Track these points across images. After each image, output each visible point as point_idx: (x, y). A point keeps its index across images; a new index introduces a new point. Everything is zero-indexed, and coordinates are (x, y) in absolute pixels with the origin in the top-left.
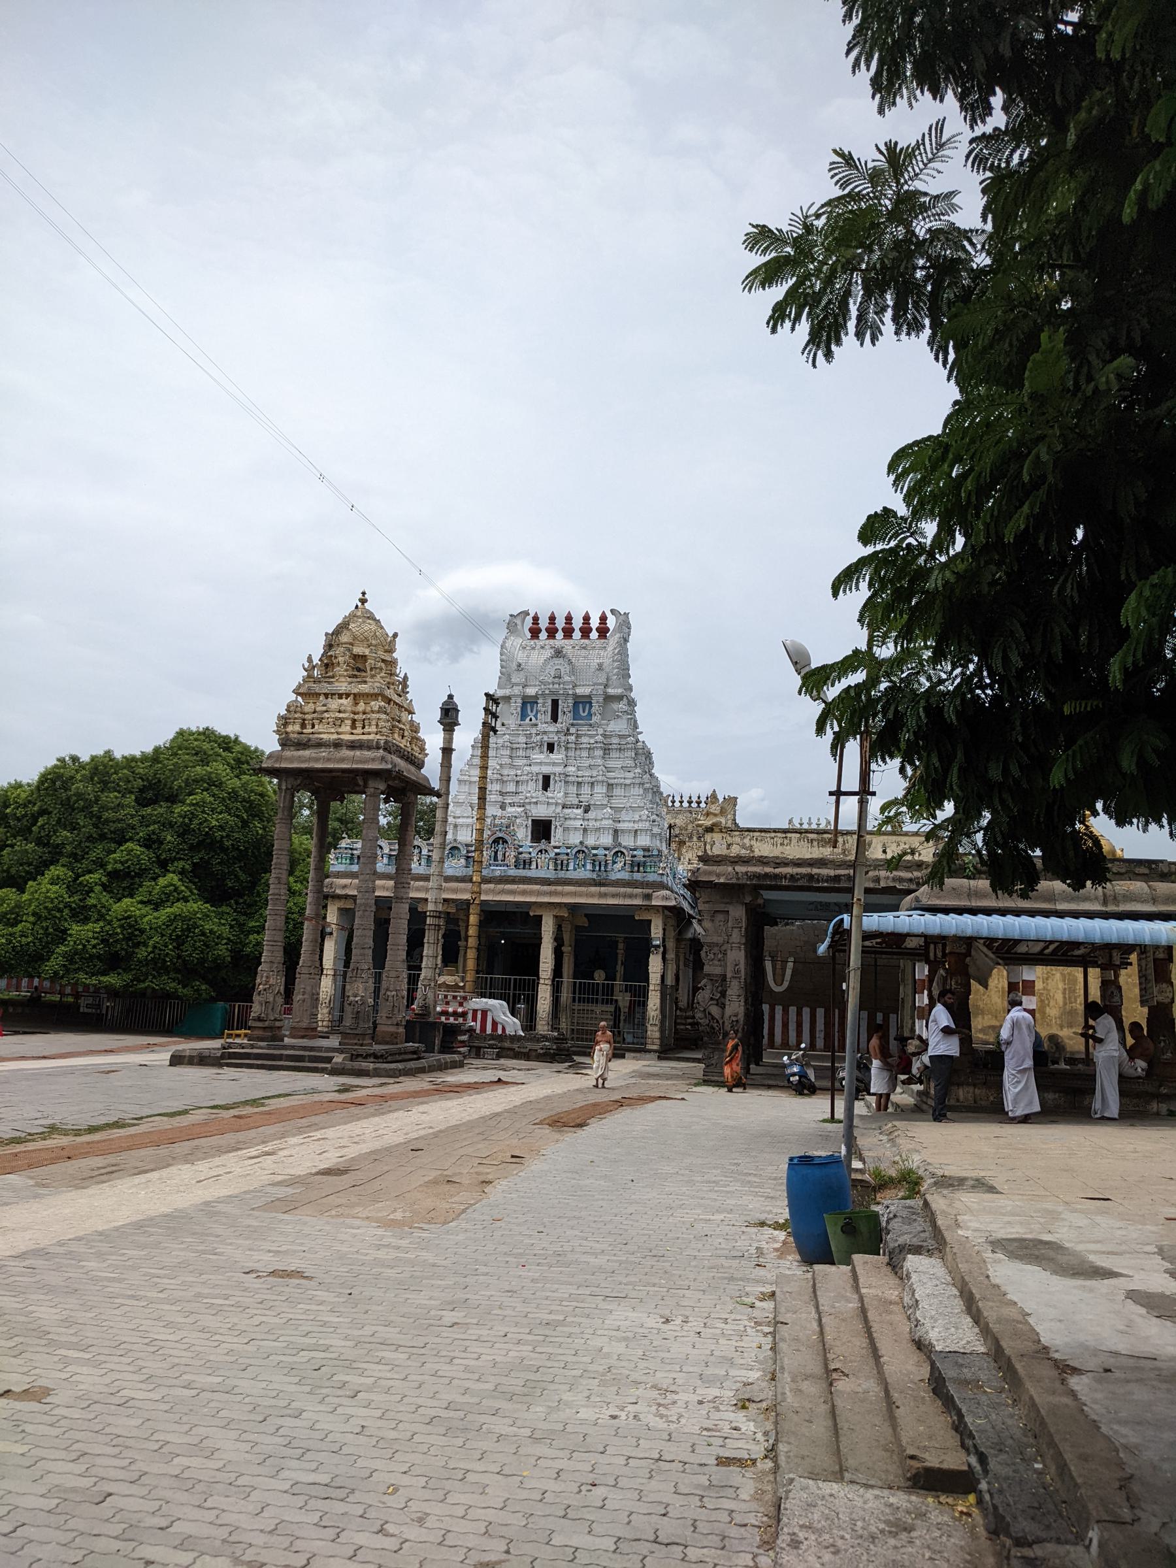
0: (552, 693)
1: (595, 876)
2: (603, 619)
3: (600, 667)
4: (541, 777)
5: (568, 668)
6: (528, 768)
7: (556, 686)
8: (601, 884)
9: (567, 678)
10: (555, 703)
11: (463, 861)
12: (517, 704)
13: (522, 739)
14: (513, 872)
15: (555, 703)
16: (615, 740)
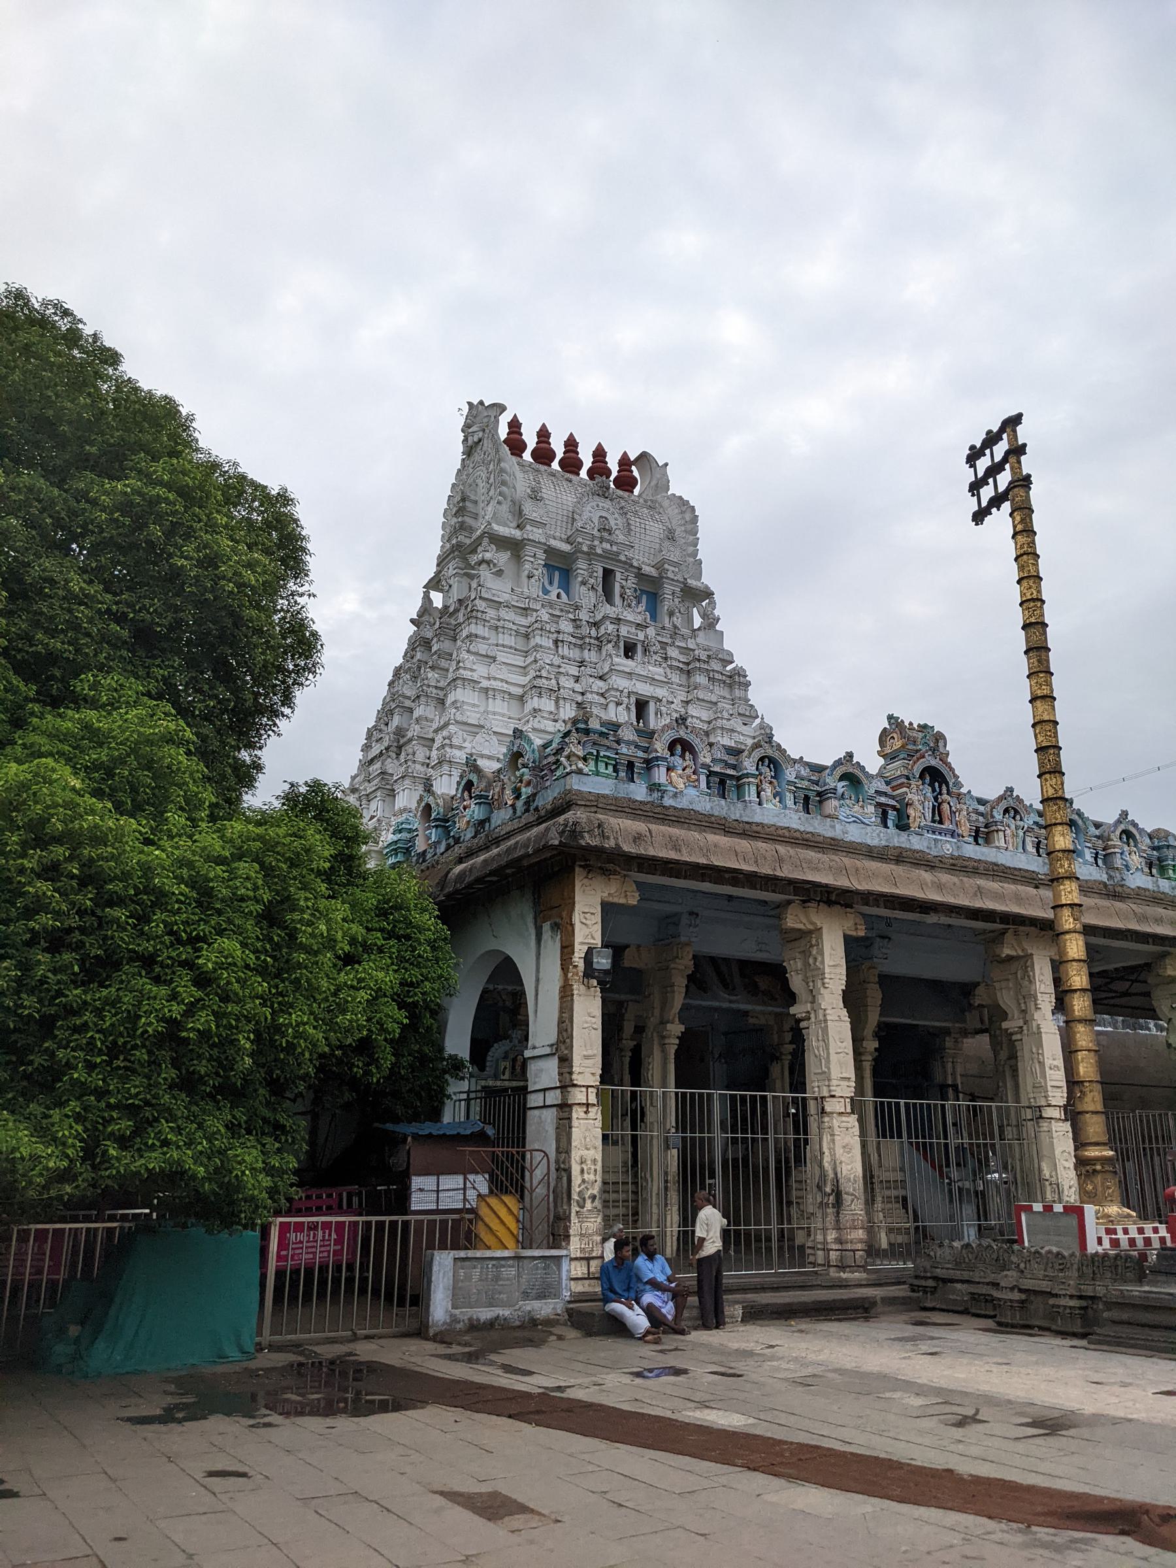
0: (607, 556)
1: (1104, 878)
2: (625, 462)
3: (671, 536)
4: (633, 700)
5: (621, 521)
6: (600, 683)
7: (608, 546)
8: (1115, 893)
9: (621, 538)
10: (608, 574)
11: (871, 809)
12: (534, 561)
13: (566, 626)
14: (971, 850)
15: (608, 574)
16: (715, 665)
